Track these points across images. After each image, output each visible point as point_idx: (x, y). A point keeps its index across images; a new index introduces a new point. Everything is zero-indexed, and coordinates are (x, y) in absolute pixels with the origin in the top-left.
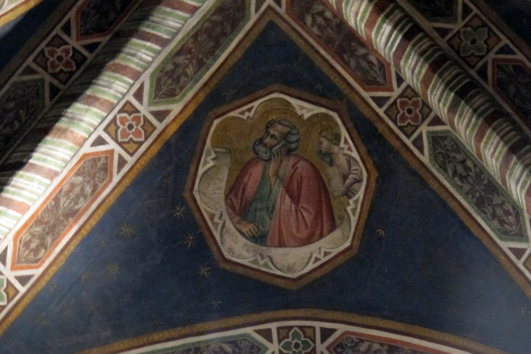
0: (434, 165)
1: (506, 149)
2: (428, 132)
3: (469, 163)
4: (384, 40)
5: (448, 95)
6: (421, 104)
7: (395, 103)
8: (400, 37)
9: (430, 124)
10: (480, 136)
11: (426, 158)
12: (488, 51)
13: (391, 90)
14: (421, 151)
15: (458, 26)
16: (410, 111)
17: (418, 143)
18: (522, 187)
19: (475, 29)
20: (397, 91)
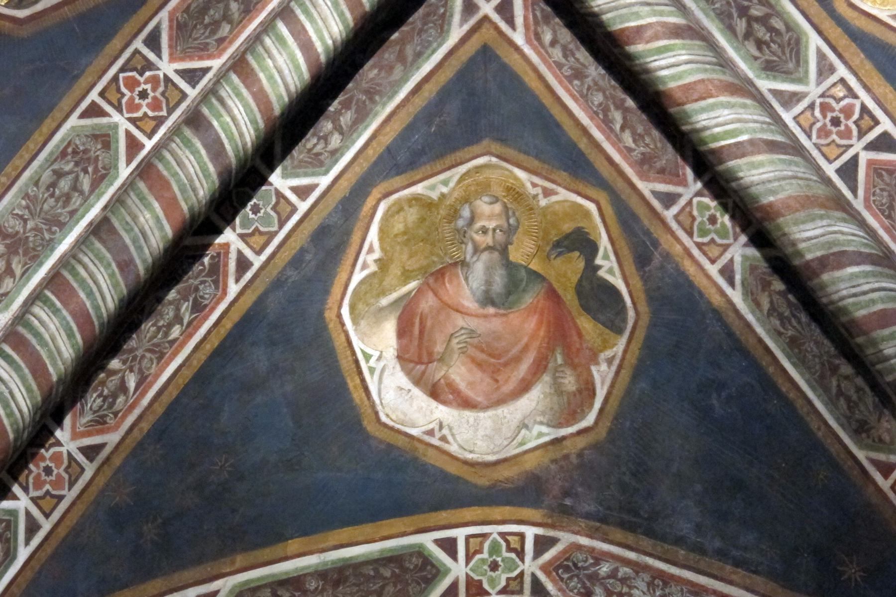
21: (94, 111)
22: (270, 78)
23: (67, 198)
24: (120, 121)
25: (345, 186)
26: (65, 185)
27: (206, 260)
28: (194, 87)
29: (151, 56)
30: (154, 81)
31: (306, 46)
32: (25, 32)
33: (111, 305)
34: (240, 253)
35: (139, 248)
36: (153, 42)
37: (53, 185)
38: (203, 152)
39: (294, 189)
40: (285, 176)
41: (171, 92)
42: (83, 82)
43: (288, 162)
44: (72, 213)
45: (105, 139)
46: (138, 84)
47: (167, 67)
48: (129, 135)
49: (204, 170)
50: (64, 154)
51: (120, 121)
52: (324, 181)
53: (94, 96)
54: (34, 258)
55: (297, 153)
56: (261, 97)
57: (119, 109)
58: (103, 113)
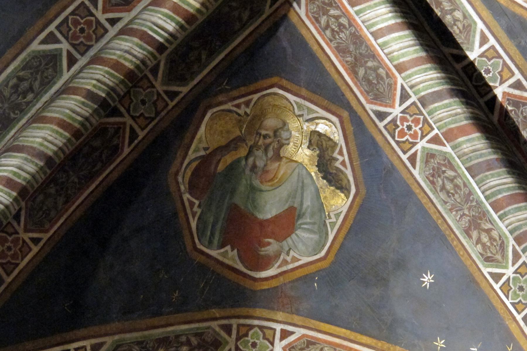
0: (29, 55)
1: (50, 153)
2: (61, 49)
3: (30, 96)
4: (160, 22)
5: (103, 90)
6: (88, 43)
7: (92, 15)
8: (161, 40)
9: (69, 53)
10: (62, 124)
11: (36, 46)
12: (133, 118)
13: (105, 11)
14: (43, 42)
15: (160, 87)
16: (82, 30)
17: (51, 39)
18: (15, 174)
19: (155, 103)
20: (102, 17)
21: (413, 159)
22: (403, 55)
23: (456, 186)
24: (422, 144)
25: (486, 13)
26: (449, 186)
27: (510, 108)
28: (410, 97)
29: (389, 119)
30: (403, 119)
31: (390, 30)
32: (363, 191)
33: (510, 180)
34: (510, 86)
35: (481, 156)
36: (381, 116)
37: (448, 193)
38: (436, 105)
39: (481, 45)
40: (472, 50)
41: (411, 111)
42: (396, 162)
43: (464, 47)
44: (465, 185)
45: (430, 156)
46: (403, 129)
47: (396, 111)
48: (429, 142)
49: (446, 106)
50: (433, 183)
51: (422, 144)
52: (480, 25)
53: (404, 157)
54: (484, 214)
55: (460, 39)
56: (416, 62)
57: (414, 144)
58: (415, 154)
